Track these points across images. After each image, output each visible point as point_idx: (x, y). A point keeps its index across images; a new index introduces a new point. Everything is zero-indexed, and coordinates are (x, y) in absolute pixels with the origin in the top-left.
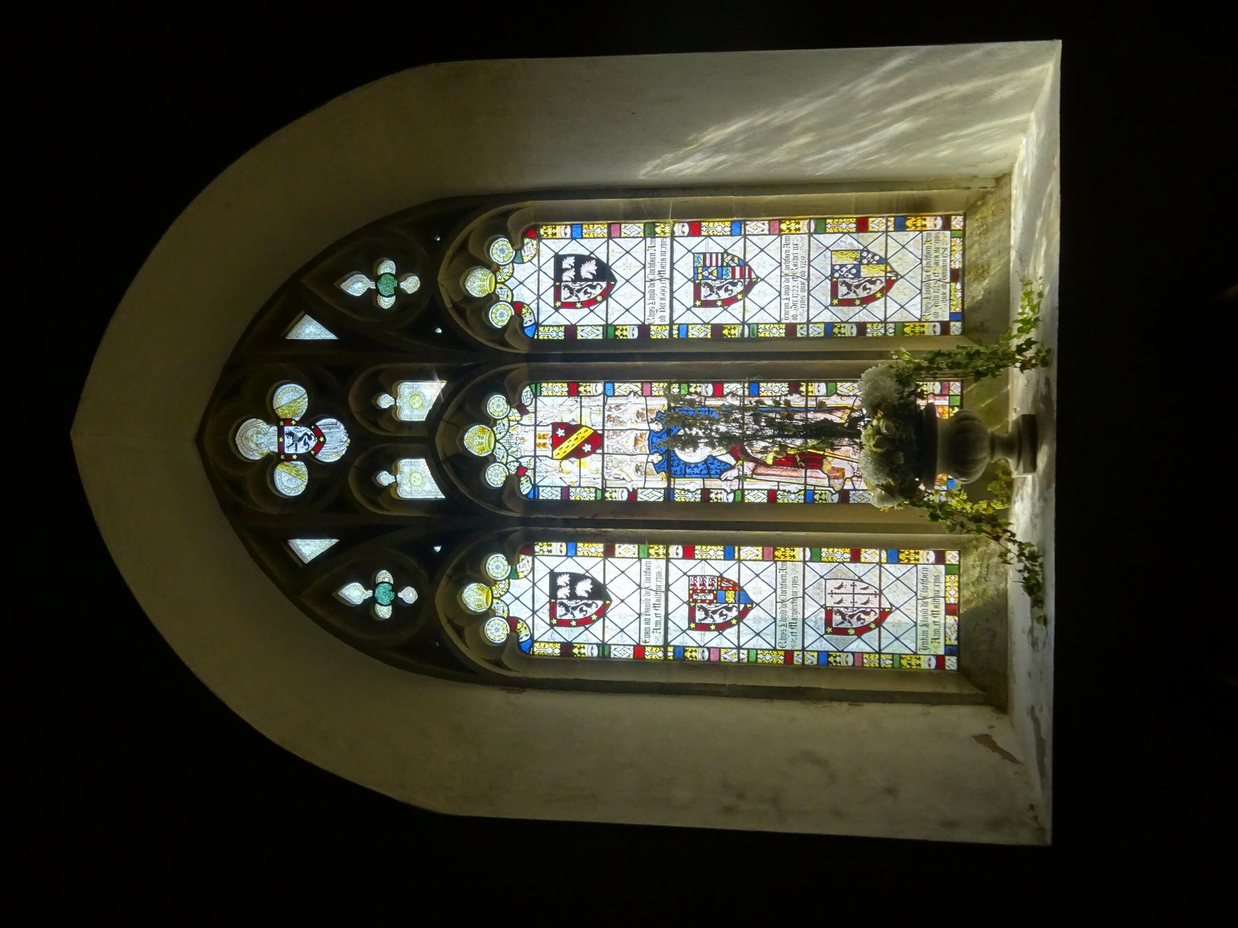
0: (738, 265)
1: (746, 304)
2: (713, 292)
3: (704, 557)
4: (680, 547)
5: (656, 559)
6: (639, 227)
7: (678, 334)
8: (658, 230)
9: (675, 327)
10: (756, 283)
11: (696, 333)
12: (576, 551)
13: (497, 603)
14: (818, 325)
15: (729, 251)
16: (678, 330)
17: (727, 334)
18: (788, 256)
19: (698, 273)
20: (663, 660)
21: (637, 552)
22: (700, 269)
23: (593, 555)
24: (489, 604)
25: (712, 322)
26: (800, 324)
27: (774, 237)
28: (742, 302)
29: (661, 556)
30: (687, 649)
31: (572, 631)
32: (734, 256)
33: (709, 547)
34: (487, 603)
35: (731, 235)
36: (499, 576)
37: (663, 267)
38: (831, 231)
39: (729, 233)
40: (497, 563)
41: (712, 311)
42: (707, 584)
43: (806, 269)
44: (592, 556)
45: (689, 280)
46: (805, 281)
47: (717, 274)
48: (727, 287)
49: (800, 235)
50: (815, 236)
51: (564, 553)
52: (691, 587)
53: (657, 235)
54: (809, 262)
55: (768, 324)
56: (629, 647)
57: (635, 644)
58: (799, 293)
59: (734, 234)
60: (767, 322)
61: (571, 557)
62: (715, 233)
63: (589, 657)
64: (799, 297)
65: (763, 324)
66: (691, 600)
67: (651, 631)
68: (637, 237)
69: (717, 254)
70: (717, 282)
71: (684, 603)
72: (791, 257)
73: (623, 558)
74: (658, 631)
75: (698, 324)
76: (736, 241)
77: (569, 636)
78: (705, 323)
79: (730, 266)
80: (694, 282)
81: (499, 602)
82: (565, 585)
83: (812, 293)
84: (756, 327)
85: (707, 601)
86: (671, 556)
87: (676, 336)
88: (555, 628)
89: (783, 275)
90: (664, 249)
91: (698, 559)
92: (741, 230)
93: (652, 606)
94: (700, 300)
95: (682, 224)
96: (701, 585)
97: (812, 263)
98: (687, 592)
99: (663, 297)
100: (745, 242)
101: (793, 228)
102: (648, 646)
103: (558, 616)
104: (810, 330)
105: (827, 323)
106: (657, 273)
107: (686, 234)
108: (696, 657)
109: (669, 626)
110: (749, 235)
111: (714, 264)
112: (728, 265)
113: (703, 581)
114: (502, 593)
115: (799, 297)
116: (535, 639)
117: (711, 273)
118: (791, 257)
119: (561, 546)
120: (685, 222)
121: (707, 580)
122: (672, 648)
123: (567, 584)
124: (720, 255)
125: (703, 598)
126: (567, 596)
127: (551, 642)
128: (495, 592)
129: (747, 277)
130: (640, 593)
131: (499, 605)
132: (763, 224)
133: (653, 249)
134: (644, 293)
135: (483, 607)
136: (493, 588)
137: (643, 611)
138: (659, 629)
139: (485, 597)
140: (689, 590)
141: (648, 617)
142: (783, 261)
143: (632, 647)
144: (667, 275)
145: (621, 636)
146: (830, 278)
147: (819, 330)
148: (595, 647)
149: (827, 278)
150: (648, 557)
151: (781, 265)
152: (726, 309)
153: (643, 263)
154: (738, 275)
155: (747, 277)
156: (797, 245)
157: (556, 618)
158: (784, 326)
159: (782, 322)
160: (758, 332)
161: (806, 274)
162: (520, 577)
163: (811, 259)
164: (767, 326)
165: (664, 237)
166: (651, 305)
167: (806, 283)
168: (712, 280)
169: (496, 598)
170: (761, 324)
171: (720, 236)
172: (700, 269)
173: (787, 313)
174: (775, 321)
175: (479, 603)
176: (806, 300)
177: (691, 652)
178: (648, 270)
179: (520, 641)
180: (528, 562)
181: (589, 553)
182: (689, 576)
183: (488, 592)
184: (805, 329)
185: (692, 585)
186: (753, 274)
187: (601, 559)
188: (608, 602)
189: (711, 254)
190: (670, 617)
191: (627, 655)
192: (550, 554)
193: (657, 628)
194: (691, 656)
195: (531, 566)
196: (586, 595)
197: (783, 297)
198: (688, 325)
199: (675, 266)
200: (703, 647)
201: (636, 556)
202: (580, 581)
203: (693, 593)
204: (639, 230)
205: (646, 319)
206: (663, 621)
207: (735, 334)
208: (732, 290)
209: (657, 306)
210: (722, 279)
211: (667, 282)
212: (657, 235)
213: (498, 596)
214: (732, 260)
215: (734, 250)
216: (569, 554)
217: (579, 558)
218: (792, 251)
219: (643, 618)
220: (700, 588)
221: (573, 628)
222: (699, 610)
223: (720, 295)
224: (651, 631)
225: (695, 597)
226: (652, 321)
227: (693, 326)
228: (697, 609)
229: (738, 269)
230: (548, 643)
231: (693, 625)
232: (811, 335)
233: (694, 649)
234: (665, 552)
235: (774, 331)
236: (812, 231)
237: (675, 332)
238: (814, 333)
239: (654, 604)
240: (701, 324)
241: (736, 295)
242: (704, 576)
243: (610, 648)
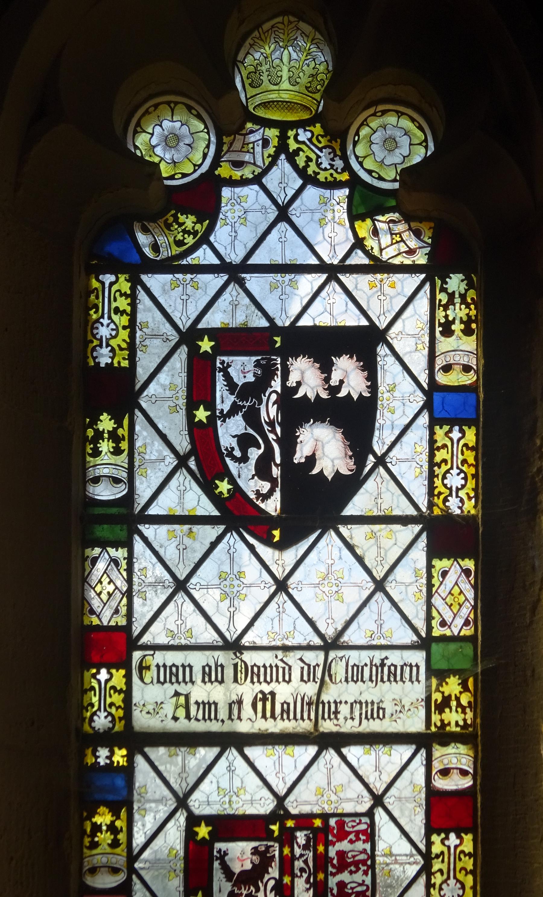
3: (437, 866)
4: (466, 783)
5: (428, 699)
12: (452, 422)
13: (266, 143)
20: (79, 730)
21: (448, 633)
23: (438, 482)
24: (261, 113)
29: (435, 718)
30: (123, 813)
31: (175, 409)
33: (469, 881)
34: (266, 105)
36: (360, 150)
40: (404, 141)
42: (345, 877)
44: (432, 476)
51: (442, 378)
52: (332, 822)
56: (123, 610)
57: (136, 629)
61: (428, 406)
63: (84, 468)
66: (290, 824)
67: (183, 689)
71: (281, 800)
73: (430, 586)
74: (181, 713)
77: (155, 400)
81: (271, 150)
82: (334, 381)
85: (287, 880)
86: (438, 751)
88: (183, 350)
91: (429, 844)
93: (266, 689)
96: (341, 854)
98: (316, 810)
102: (128, 677)
108: (94, 845)
109: (202, 751)
113: (356, 864)
114: (301, 161)
116: (144, 278)
119: (467, 369)
121: (359, 877)
122: (123, 762)
123: (338, 388)
125: (299, 864)
126: (295, 390)
127: (132, 335)
128: (303, 136)
130: (309, 648)
131: (258, 149)
135: (251, 92)
136: (318, 129)
137: (249, 657)
138: (188, 717)
139: (285, 96)
140: (325, 817)
141: (229, 672)
143: (123, 622)
145: (159, 582)
148: (120, 491)
150: (431, 672)
157: (217, 350)
162: (357, 224)
169: (283, 138)
175: (265, 78)
177: (112, 828)
179: (137, 227)
180: (411, 252)
181: (444, 468)
182: (370, 813)
183: (306, 108)
185: (341, 824)
187: (423, 503)
188: (276, 533)
190: (232, 754)
191: (96, 603)
192: (438, 329)
193: (193, 709)
194: (97, 828)
195: (397, 261)
196: (299, 457)
200: (132, 870)
201: (437, 632)
202: (347, 435)
203: (315, 831)
206: (214, 727)
213: (293, 146)
216: (437, 397)
217: (426, 434)
219: (223, 657)
220: (332, 852)
221: (183, 412)
222: (255, 851)
224: (183, 689)
225: (301, 837)
228: (261, 845)
230: (132, 326)
231: (203, 831)
233: (122, 837)
234: (453, 728)
239: (273, 694)
242: (373, 867)
243: (116, 545)
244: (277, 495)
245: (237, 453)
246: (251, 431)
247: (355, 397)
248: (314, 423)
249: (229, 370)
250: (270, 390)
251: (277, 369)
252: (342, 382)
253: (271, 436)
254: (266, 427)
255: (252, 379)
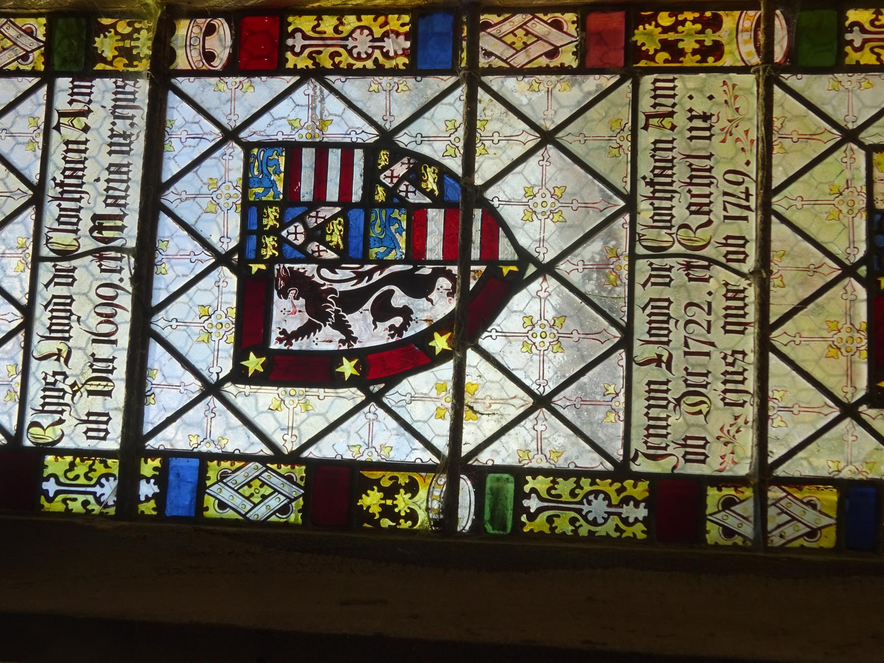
0: (437, 203)
1: (470, 379)
2: (324, 317)
6: (30, 33)
7: (160, 498)
8: (106, 46)
9: (148, 467)
10: (517, 283)
11: (237, 501)
14: (806, 493)
15: (403, 139)
16: (161, 478)
17: (375, 510)
18: (664, 168)
19: (261, 232)
22: (272, 213)
25: (313, 453)
26: (719, 481)
27: (607, 81)
28: (446, 371)
32: (420, 162)
35: (413, 70)
37: (114, 201)
38: (867, 58)
39: (402, 61)
41: (313, 400)
43: (750, 228)
45: (222, 259)
46: (743, 283)
47: (345, 238)
48: (392, 292)
49: (721, 77)
50: (791, 80)
53: (100, 67)
54: (768, 191)
55: (565, 474)
58: (717, 336)
59: (421, 66)
60: (561, 464)
62: (345, 60)
64: (716, 355)
65: (545, 472)
68: (18, 73)
69: (347, 150)
70: (341, 274)
72: (681, 173)
75: (247, 458)
76: (431, 94)
78: (278, 456)
79: (403, 203)
80: (240, 270)
83: (778, 337)
84: (511, 486)
87: (148, 508)
89: (640, 250)
90: (121, 126)
92: (457, 49)
94: (262, 349)
95: (202, 22)
97: (778, 203)
99: (106, 328)
100: (471, 101)
101: (689, 45)
104: (774, 517)
105: (851, 482)
106: (86, 224)
107: (218, 64)
110: (492, 71)
111: (333, 192)
112: (394, 200)
115: (716, 355)
117: (317, 234)
118: (681, 173)
120: (215, 13)
124: (359, 154)
129: (475, 254)
132: (557, 25)
133: (80, 122)
134: (27, 311)
142: (643, 190)
144: (130, 237)
146: (863, 271)
147: (810, 517)
149: (848, 271)
151: (631, 206)
152: (377, 399)
153: (35, 178)
154: (434, 247)
155: (475, 254)
156: (705, 117)
158: (641, 490)
159: (634, 468)
160: (520, 509)
161: (752, 249)
163: (775, 184)
164: (564, 487)
165: (125, 76)
166: (51, 366)
167: (751, 294)
168: (323, 264)
170: (535, 472)
171: (363, 73)
172: (272, 213)
173: (655, 427)
174: (591, 461)
176: (751, 375)
178: (52, 210)
184: (747, 508)
186: (504, 243)
189: (322, 149)
197: (641, 351)
198: (205, 458)
199: (170, 198)
204: (27, 42)
205: (29, 419)
207: (412, 516)
208: (406, 313)
209: (78, 365)
210: (365, 260)
211: (128, 265)
212: (100, 67)
214: (415, 177)
215: (424, 139)
218: (681, 146)
223: (356, 330)
226: (51, 435)
227: (226, 464)
229: (436, 219)
232: (776, 541)
235: (598, 507)
236: (779, 55)
237: (147, 489)
238: (790, 531)
240: (262, 460)
241: (426, 335)
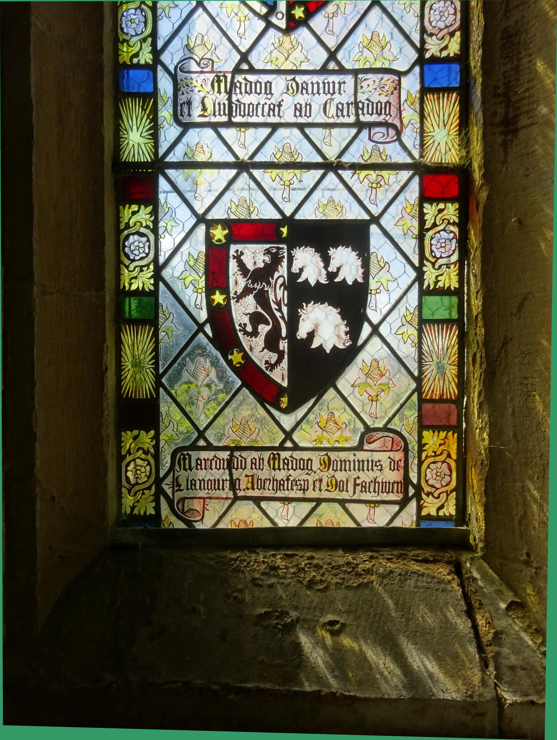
82: (332, 268)
103: (240, 247)
123: (335, 275)
126: (299, 275)
196: (302, 333)
244: (285, 363)
245: (249, 329)
246: (260, 310)
247: (350, 282)
248: (314, 304)
249: (242, 258)
250: (276, 275)
251: (283, 257)
252: (339, 269)
253: (278, 314)
254: (274, 306)
255: (262, 265)
